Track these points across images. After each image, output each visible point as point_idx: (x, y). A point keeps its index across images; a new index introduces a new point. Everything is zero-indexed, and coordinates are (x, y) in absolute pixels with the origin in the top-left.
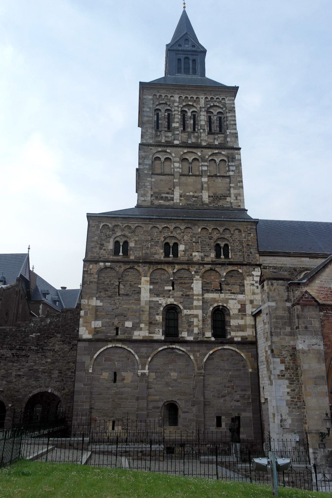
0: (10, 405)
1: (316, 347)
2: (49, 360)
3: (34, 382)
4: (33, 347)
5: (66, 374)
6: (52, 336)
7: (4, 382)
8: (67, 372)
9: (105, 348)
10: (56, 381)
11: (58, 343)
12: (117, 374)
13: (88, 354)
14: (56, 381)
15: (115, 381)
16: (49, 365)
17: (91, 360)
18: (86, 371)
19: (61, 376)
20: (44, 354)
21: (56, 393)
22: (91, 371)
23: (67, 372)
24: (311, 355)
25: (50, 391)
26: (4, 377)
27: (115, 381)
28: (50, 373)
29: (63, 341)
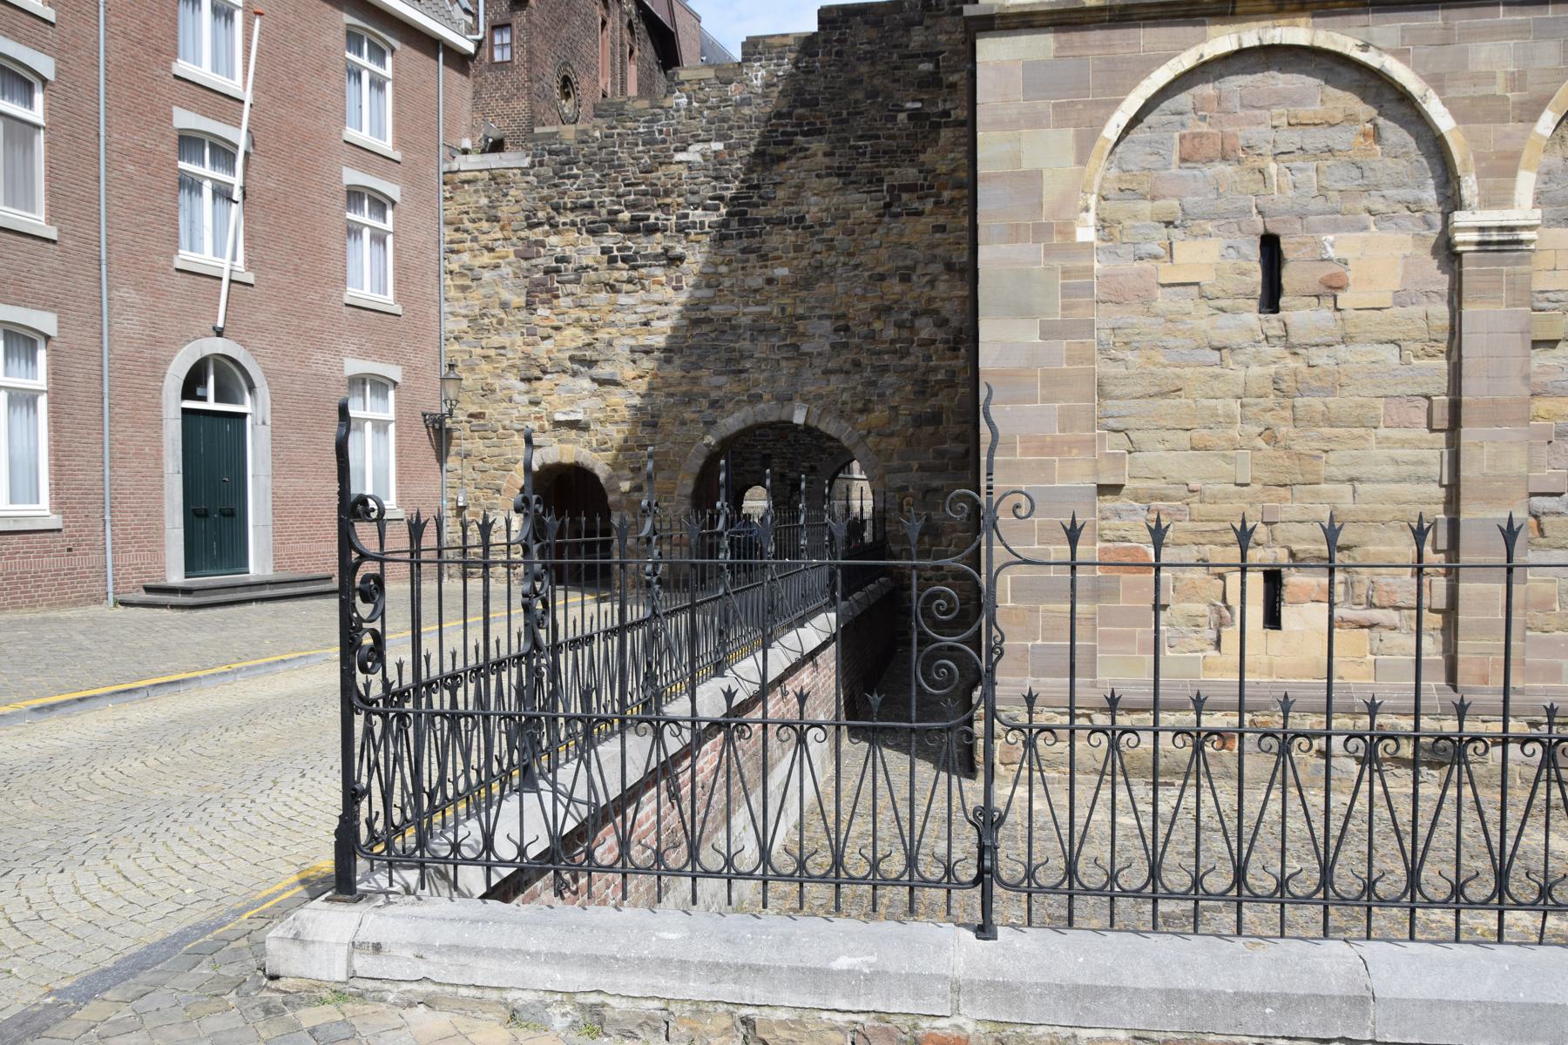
0: (625, 486)
2: (781, 272)
3: (722, 379)
4: (696, 215)
5: (872, 336)
6: (782, 150)
7: (586, 383)
8: (877, 325)
9: (1187, 61)
10: (827, 372)
11: (814, 182)
12: (1285, 244)
13: (1062, 116)
14: (827, 372)
15: (1271, 298)
16: (783, 293)
17: (1082, 158)
18: (1051, 234)
19: (845, 345)
20: (755, 242)
21: (830, 426)
22: (1086, 233)
23: (877, 325)
25: (799, 418)
26: (583, 361)
27: (1271, 298)
28: (793, 330)
29: (841, 173)
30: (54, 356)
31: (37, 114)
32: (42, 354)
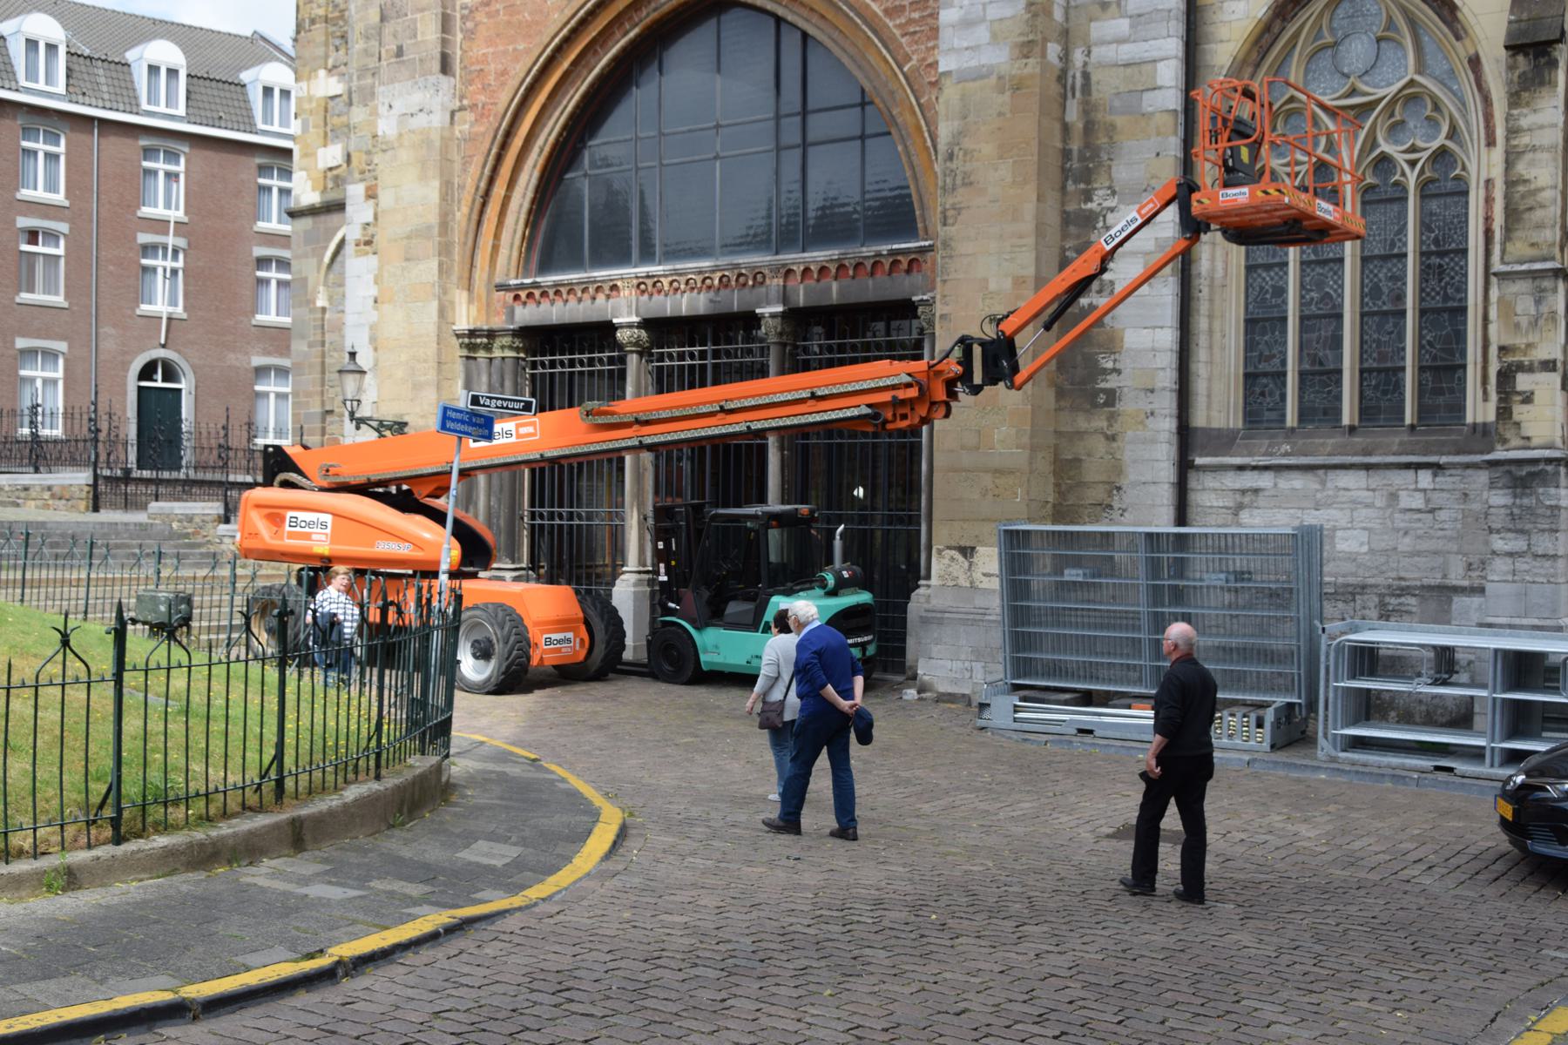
1: (421, 121)
24: (404, 155)
30: (66, 361)
31: (60, 251)
32: (61, 362)
